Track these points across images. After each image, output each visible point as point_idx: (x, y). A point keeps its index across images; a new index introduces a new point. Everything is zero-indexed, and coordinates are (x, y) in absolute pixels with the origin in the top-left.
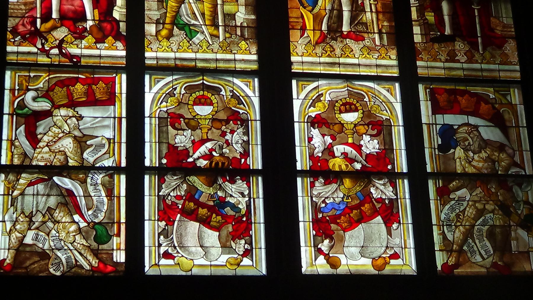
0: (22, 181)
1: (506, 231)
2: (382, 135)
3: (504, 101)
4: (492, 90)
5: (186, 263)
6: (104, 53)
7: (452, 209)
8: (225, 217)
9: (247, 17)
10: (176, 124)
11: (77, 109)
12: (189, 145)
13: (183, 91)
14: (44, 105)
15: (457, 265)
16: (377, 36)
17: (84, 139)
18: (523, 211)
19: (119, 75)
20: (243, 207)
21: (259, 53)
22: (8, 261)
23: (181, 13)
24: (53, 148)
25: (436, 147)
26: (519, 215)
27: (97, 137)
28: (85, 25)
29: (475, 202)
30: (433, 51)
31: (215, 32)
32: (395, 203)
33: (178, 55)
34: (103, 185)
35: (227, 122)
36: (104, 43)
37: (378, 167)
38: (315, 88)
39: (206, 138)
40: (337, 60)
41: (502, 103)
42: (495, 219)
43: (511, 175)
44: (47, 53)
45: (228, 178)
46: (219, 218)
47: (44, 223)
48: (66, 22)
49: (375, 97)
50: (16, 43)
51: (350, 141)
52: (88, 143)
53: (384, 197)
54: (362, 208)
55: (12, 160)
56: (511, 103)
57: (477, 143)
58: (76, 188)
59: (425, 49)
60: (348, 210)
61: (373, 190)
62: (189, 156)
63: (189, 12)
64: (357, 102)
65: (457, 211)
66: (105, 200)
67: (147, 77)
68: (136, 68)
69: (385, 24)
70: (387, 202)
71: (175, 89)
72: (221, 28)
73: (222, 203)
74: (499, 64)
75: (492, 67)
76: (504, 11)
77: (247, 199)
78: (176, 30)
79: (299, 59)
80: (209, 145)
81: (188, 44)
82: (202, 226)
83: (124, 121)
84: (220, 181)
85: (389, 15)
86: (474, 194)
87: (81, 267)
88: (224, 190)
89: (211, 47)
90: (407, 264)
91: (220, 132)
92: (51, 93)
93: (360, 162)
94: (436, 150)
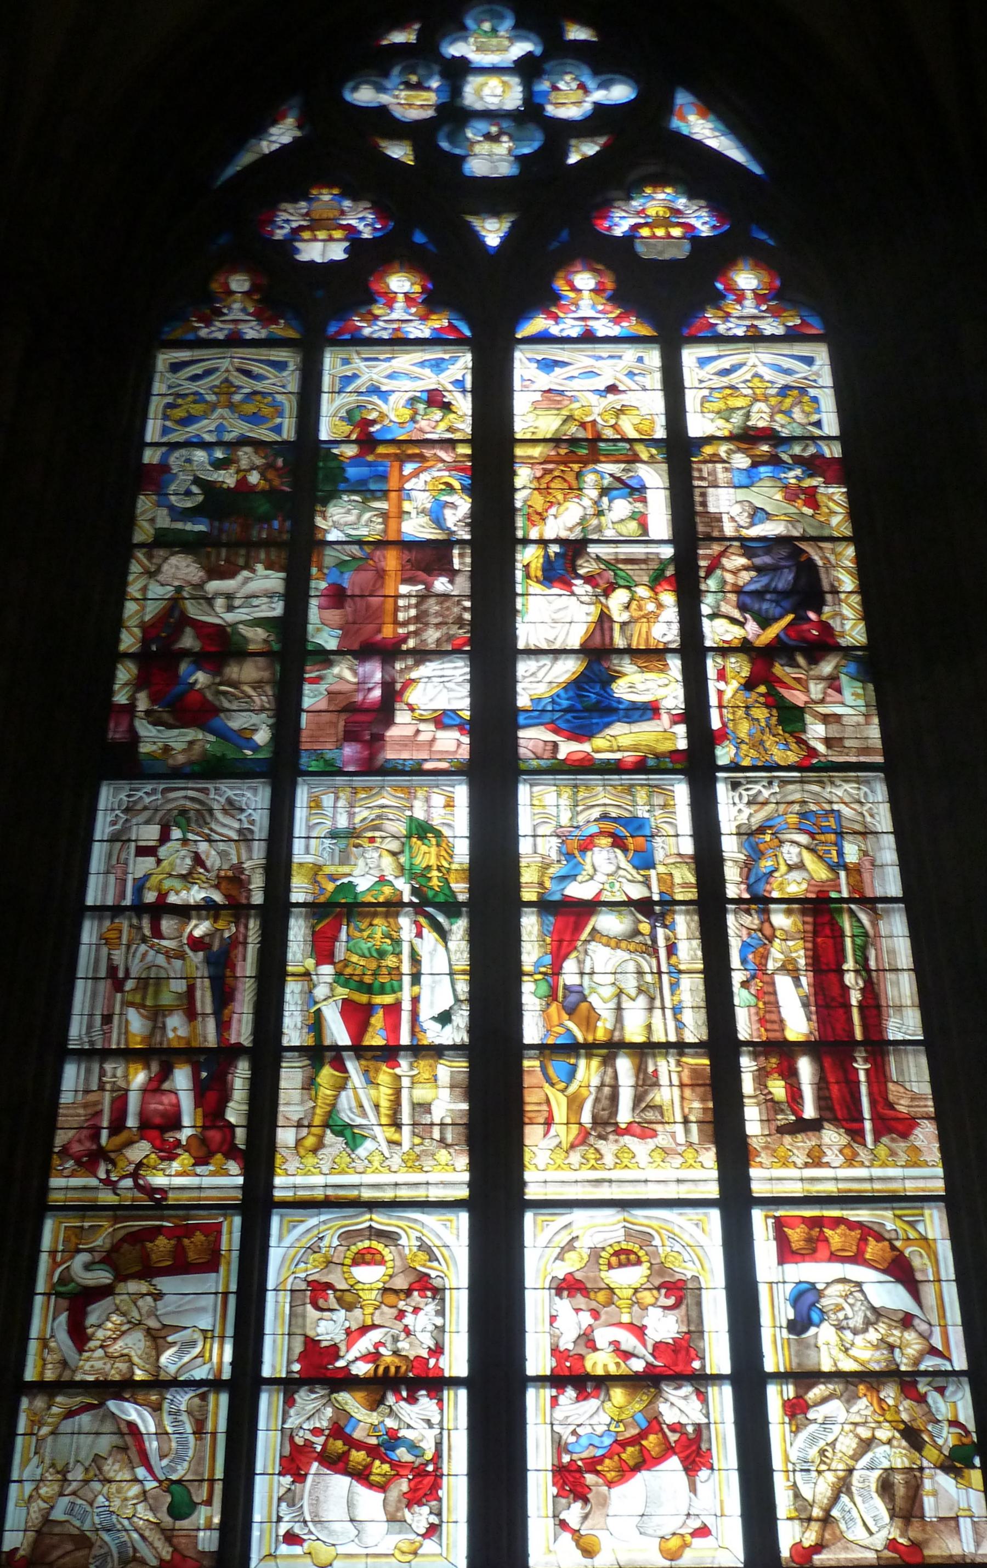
0: (55, 1410)
2: (683, 1307)
3: (912, 1235)
4: (889, 1214)
6: (207, 1181)
7: (813, 1439)
9: (453, 1106)
10: (321, 1302)
11: (156, 1281)
12: (340, 1337)
14: (103, 1277)
15: (819, 1547)
16: (679, 1129)
17: (163, 1333)
18: (947, 1438)
19: (229, 1219)
22: (22, 1552)
23: (339, 1107)
24: (111, 1350)
25: (784, 1324)
26: (939, 1448)
27: (185, 1328)
28: (178, 1136)
29: (856, 1424)
30: (782, 1149)
31: (396, 1137)
32: (705, 1432)
34: (189, 1412)
35: (408, 1293)
36: (207, 1164)
39: (369, 1322)
42: (892, 1455)
43: (926, 1373)
45: (404, 1394)
46: (386, 1467)
47: (86, 1482)
49: (674, 1237)
50: (66, 1173)
51: (626, 1319)
52: (170, 1339)
53: (684, 1420)
54: (644, 1443)
55: (42, 1373)
57: (861, 1314)
58: (144, 1421)
59: (766, 1148)
60: (617, 1448)
61: (663, 1408)
62: (338, 1357)
63: (354, 1104)
64: (641, 1248)
65: (822, 1444)
66: (191, 1438)
68: (258, 1204)
69: (697, 1105)
70: (690, 1429)
71: (321, 1239)
72: (406, 1130)
73: (393, 1439)
74: (902, 1166)
75: (891, 1172)
76: (913, 1070)
78: (329, 1137)
80: (374, 1336)
81: (349, 1160)
82: (354, 1483)
83: (232, 1300)
84: (391, 1399)
85: (702, 1089)
86: (854, 1409)
89: (387, 1163)
91: (394, 1312)
92: (114, 1255)
93: (643, 1358)
94: (785, 1331)
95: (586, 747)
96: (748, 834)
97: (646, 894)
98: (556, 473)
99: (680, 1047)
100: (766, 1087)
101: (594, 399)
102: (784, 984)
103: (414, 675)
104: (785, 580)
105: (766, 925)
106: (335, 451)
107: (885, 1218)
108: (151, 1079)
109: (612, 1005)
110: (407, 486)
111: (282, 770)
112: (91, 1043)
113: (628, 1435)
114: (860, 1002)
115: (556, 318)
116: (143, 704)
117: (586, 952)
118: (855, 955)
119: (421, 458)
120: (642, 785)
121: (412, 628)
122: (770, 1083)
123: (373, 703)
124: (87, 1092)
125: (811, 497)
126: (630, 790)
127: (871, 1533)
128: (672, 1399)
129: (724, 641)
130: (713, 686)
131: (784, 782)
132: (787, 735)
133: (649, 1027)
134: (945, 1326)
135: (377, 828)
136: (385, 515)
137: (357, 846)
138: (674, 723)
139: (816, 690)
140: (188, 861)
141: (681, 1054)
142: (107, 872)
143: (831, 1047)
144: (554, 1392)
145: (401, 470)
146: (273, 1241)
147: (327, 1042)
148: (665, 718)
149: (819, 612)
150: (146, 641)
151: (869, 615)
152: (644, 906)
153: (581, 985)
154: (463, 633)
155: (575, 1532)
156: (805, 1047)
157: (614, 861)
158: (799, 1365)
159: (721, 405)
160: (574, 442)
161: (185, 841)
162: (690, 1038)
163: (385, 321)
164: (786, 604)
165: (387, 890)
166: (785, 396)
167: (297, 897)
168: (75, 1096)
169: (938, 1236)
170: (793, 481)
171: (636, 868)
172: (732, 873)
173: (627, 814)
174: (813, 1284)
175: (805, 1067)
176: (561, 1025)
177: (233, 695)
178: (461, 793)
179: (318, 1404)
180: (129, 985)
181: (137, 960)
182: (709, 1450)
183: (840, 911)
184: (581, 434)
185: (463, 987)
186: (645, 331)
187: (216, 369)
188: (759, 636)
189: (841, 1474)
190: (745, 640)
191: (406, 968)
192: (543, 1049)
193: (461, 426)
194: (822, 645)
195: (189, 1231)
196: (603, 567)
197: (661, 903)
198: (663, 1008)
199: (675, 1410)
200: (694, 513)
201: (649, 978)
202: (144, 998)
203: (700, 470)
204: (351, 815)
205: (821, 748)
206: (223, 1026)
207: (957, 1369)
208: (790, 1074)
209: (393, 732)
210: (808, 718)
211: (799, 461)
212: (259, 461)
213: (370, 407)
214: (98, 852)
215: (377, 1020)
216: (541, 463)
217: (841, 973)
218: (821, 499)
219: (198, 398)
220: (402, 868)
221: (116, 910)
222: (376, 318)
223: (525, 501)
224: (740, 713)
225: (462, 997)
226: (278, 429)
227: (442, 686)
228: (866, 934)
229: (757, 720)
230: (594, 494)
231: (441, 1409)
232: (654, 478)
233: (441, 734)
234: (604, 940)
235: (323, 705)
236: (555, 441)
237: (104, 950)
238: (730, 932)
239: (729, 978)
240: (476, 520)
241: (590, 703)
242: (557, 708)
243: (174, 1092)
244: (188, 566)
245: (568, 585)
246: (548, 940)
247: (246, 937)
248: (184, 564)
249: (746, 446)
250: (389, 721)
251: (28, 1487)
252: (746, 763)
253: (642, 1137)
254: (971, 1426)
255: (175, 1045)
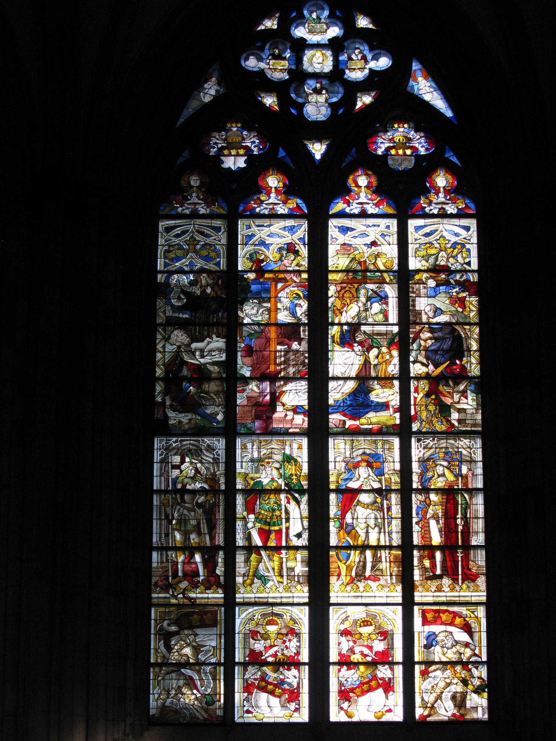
0: (162, 672)
1: (464, 696)
3: (472, 615)
4: (465, 608)
5: (260, 716)
6: (210, 596)
7: (430, 683)
8: (284, 690)
10: (255, 637)
11: (195, 630)
12: (262, 649)
13: (259, 617)
15: (429, 716)
16: (389, 578)
17: (199, 647)
18: (477, 682)
20: (295, 685)
21: (310, 591)
26: (474, 686)
29: (445, 678)
30: (427, 585)
31: (281, 580)
32: (392, 681)
33: (257, 595)
34: (210, 673)
35: (287, 635)
37: (384, 658)
38: (345, 612)
40: (360, 594)
41: (471, 617)
43: (472, 662)
44: (176, 597)
46: (280, 690)
48: (187, 578)
49: (384, 616)
50: (157, 592)
51: (366, 644)
53: (385, 676)
56: (477, 617)
57: (451, 643)
60: (361, 685)
61: (378, 673)
62: (262, 656)
63: (264, 568)
65: (433, 684)
66: (212, 681)
67: (237, 609)
68: (230, 604)
69: (396, 569)
70: (387, 679)
71: (255, 616)
72: (285, 578)
73: (283, 682)
76: (479, 557)
77: (298, 679)
78: (256, 580)
79: (336, 595)
80: (275, 649)
81: (263, 588)
84: (281, 669)
87: (198, 718)
88: (284, 675)
90: (398, 716)
91: (282, 641)
95: (357, 423)
96: (423, 461)
97: (380, 486)
98: (347, 289)
99: (391, 547)
100: (423, 562)
101: (365, 248)
102: (433, 523)
103: (284, 389)
104: (447, 345)
105: (427, 499)
106: (245, 276)
107: (463, 610)
108: (186, 558)
109: (365, 531)
110: (279, 295)
111: (230, 431)
112: (162, 544)
113: (365, 681)
114: (462, 530)
115: (348, 203)
116: (168, 403)
117: (355, 510)
118: (461, 511)
119: (284, 280)
120: (380, 440)
121: (282, 366)
122: (424, 561)
123: (267, 402)
124: (162, 563)
125: (462, 302)
126: (375, 442)
127: (447, 712)
128: (381, 670)
129: (418, 374)
130: (413, 395)
131: (439, 439)
132: (442, 418)
133: (379, 540)
134: (481, 647)
135: (271, 458)
136: (269, 310)
137: (262, 465)
138: (395, 412)
139: (456, 397)
140: (193, 471)
141: (391, 550)
142: (160, 476)
143: (448, 548)
144: (339, 667)
145: (276, 286)
146: (237, 617)
147: (253, 545)
148: (391, 409)
149: (461, 361)
150: (166, 372)
151: (482, 362)
152: (378, 491)
153: (353, 523)
154: (305, 369)
155: (345, 710)
156: (438, 548)
157: (367, 473)
158: (427, 659)
159: (423, 253)
160: (355, 272)
161: (191, 463)
162: (394, 544)
163: (266, 204)
164: (447, 356)
165: (275, 484)
166: (455, 248)
167: (239, 487)
168: (158, 564)
169: (482, 616)
170: (454, 294)
171: (377, 476)
172: (415, 478)
173: (373, 452)
174: (434, 633)
175: (438, 555)
176: (344, 538)
177: (206, 397)
178: (305, 441)
179: (256, 670)
180: (174, 522)
181: (176, 512)
182: (393, 686)
183: (458, 494)
184: (359, 268)
185: (306, 523)
186: (390, 211)
187: (188, 231)
188: (433, 371)
189: (439, 693)
190: (428, 373)
191: (283, 516)
192: (337, 548)
193: (303, 263)
194: (461, 376)
195: (206, 613)
196: (367, 337)
197: (386, 490)
198: (385, 532)
199: (382, 673)
200: (409, 310)
201: (379, 520)
202: (180, 527)
203: (413, 288)
204: (259, 452)
205: (456, 424)
206: (212, 538)
207: (483, 660)
208: (432, 558)
209: (276, 415)
210: (452, 411)
211: (458, 283)
212: (210, 282)
213: (261, 252)
214: (156, 466)
215: (273, 536)
216: (340, 284)
217: (456, 519)
218: (467, 304)
219: (180, 248)
220: (281, 475)
221: (166, 492)
222: (262, 202)
223: (333, 304)
224: (423, 408)
225: (306, 527)
226: (218, 264)
227: (296, 394)
228: (467, 503)
229: (431, 411)
230: (363, 299)
231: (299, 673)
232: (391, 291)
233: (296, 416)
234: (362, 505)
235: (245, 403)
236: (346, 271)
237: (163, 508)
238: (413, 502)
239: (412, 520)
240: (310, 313)
241: (359, 403)
242: (345, 405)
243: (196, 563)
244: (182, 335)
245: (351, 347)
246: (340, 505)
247: (219, 503)
248: (180, 334)
249: (434, 275)
250: (274, 411)
251: (156, 696)
252: (424, 430)
253: (374, 581)
254: (486, 679)
255: (194, 545)
